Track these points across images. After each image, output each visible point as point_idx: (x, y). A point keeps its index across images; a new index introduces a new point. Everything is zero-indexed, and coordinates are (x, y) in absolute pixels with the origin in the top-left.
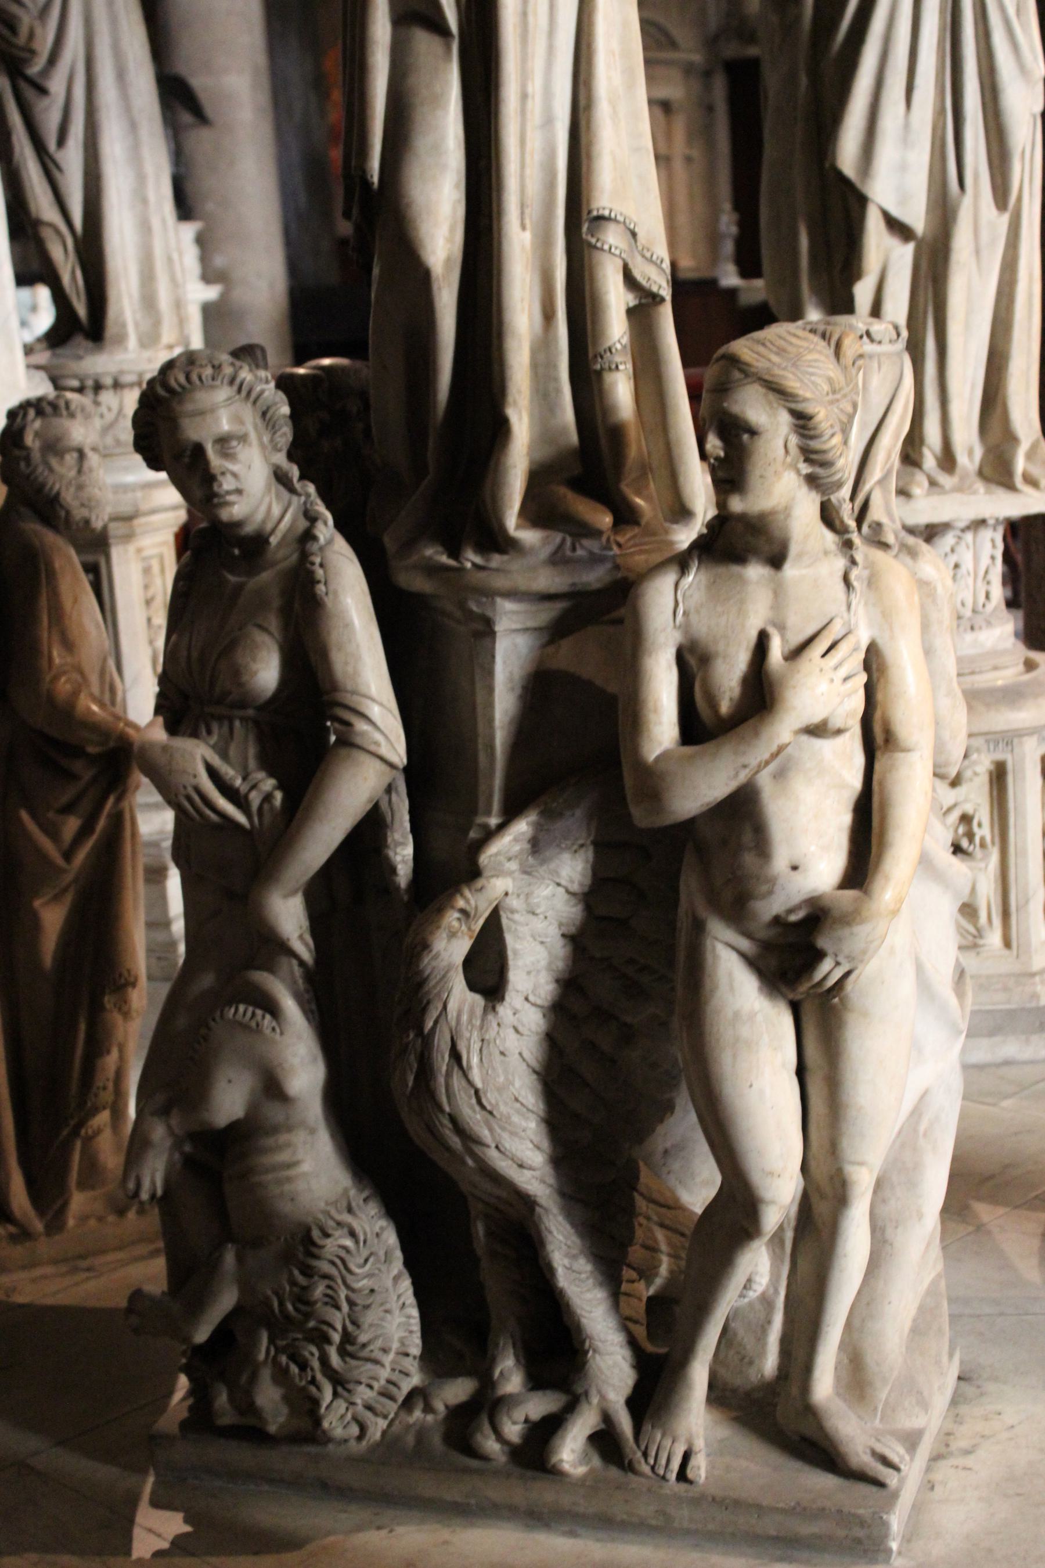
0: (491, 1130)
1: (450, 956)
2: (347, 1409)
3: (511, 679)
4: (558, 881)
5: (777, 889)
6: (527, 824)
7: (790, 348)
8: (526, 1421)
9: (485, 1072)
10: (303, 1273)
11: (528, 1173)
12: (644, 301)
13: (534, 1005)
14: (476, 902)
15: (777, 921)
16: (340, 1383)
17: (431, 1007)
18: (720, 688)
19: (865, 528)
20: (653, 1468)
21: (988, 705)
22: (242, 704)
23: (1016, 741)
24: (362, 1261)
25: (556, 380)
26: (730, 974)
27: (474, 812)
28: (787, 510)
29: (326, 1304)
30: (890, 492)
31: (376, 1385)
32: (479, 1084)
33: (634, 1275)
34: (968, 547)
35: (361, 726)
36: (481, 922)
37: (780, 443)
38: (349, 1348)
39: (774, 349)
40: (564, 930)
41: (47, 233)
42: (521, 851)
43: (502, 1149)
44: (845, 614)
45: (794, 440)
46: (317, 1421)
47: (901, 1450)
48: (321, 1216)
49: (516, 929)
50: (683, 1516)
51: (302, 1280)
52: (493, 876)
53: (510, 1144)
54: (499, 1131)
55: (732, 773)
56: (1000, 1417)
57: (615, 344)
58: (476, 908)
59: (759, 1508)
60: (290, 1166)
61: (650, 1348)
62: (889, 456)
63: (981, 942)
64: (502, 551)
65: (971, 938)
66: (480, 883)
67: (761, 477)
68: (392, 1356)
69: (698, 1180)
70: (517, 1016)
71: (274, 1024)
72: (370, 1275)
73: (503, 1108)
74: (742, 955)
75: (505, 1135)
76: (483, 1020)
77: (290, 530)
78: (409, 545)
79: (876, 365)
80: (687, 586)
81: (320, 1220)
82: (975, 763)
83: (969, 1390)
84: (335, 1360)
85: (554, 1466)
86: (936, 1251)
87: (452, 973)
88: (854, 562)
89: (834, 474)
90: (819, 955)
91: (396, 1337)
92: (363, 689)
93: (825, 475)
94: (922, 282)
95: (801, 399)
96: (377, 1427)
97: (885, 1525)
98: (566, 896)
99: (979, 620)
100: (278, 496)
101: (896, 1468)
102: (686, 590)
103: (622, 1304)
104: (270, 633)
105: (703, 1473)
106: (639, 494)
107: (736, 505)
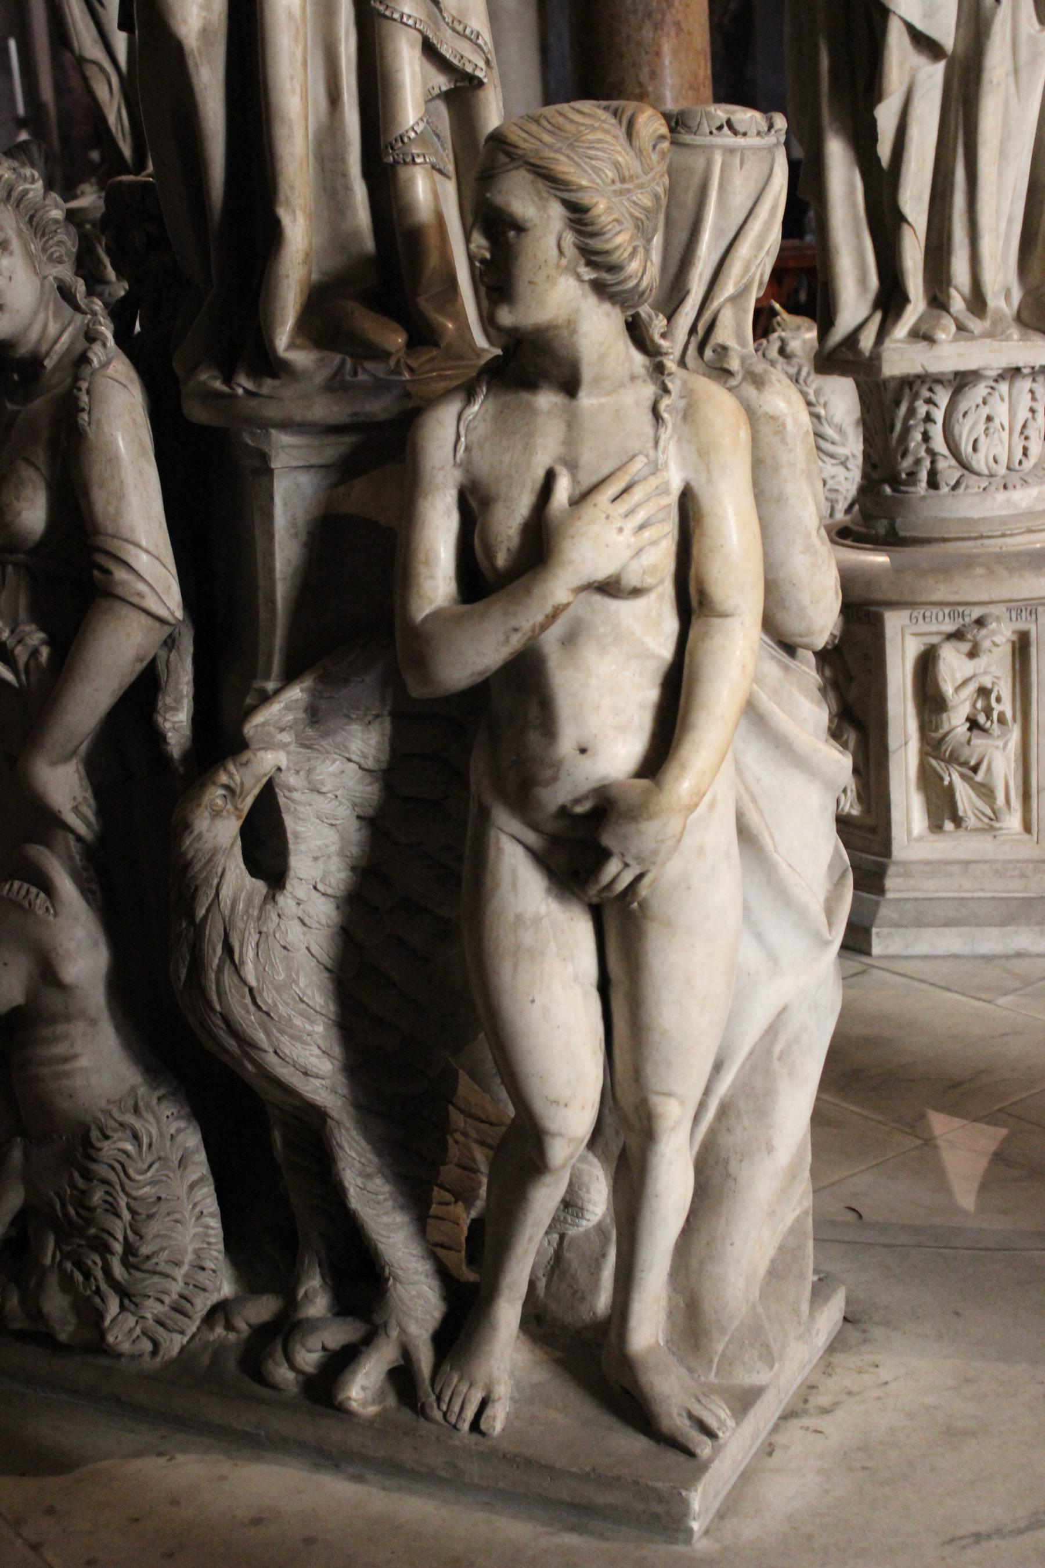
0: (268, 1033)
1: (215, 837)
2: (137, 1322)
3: (294, 525)
4: (347, 755)
6: (302, 691)
7: (569, 127)
9: (261, 968)
10: (83, 1176)
11: (317, 1082)
12: (458, 84)
13: (324, 894)
14: (241, 778)
15: (563, 811)
16: (127, 1296)
18: (497, 537)
19: (708, 353)
20: (445, 1415)
21: (1011, 570)
22: (13, 549)
24: (145, 1166)
26: (514, 871)
28: (571, 325)
29: (106, 1210)
30: (745, 311)
31: (167, 1300)
32: (253, 983)
33: (448, 1197)
34: (1002, 399)
35: (120, 574)
36: (250, 801)
37: (552, 241)
38: (131, 1259)
39: (549, 127)
40: (359, 811)
41: (91, 71)
42: (296, 722)
43: (281, 1054)
44: (652, 453)
45: (569, 238)
46: (102, 1334)
47: (724, 1413)
48: (100, 1115)
49: (296, 809)
50: (473, 1469)
51: (80, 1182)
53: (289, 1047)
54: (278, 1035)
57: (407, 132)
58: (242, 784)
59: (550, 1470)
60: (67, 1059)
62: (747, 269)
63: (997, 825)
64: (274, 375)
65: (986, 820)
66: (246, 756)
67: (531, 283)
68: (185, 1268)
70: (301, 906)
71: (48, 904)
72: (152, 1183)
73: (282, 1010)
74: (527, 848)
75: (284, 1039)
76: (262, 909)
77: (69, 350)
78: (194, 368)
79: (738, 161)
80: (471, 417)
81: (100, 1120)
82: (994, 633)
83: (853, 1334)
84: (118, 1271)
85: (341, 1404)
86: (804, 1184)
87: (221, 859)
88: (666, 390)
90: (604, 855)
91: (190, 1249)
92: (125, 533)
93: (613, 282)
94: (953, 106)
95: (574, 187)
96: (174, 1344)
97: (685, 1503)
98: (360, 773)
99: (1014, 478)
100: (57, 314)
103: (429, 1229)
104: (37, 469)
105: (498, 1426)
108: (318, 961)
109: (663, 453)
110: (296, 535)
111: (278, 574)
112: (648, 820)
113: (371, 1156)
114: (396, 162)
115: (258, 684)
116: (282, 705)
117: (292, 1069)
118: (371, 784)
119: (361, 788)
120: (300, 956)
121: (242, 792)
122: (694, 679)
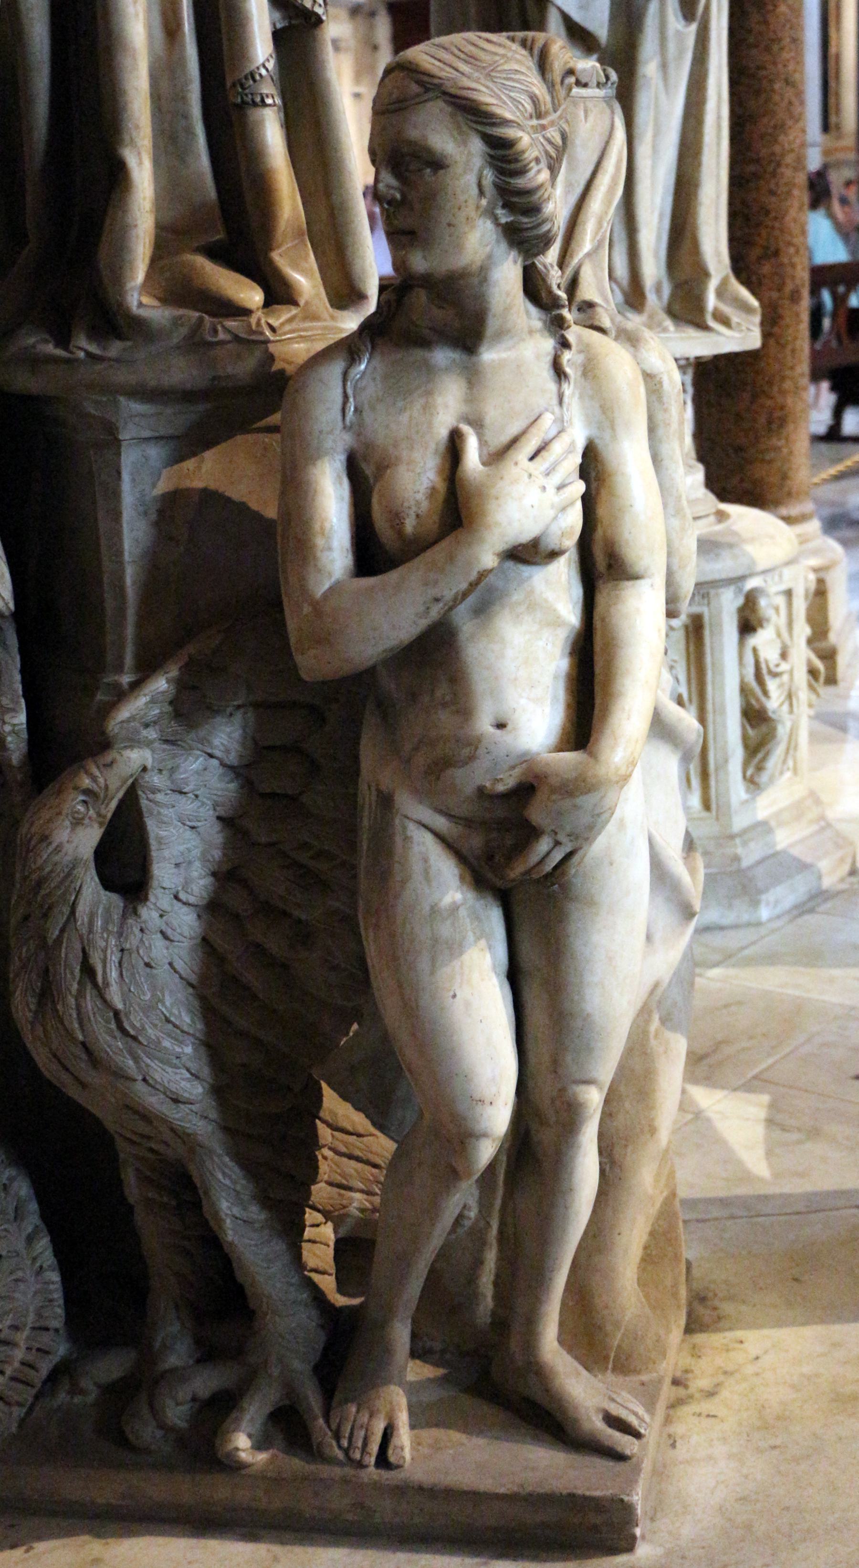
0: (136, 1059)
4: (210, 751)
5: (481, 751)
6: (167, 682)
8: (194, 1399)
9: (126, 988)
14: (106, 780)
15: (481, 792)
17: (56, 911)
20: (346, 1451)
23: (712, 592)
25: (186, 116)
26: (426, 860)
28: (483, 272)
32: (120, 1006)
33: (319, 1218)
36: (114, 804)
37: (471, 179)
39: (462, 56)
40: (221, 811)
43: (151, 1081)
44: (557, 409)
45: (489, 176)
49: (159, 813)
52: (126, 747)
53: (161, 1073)
54: (149, 1061)
55: (422, 609)
56: (742, 1346)
58: (107, 787)
61: (340, 1301)
67: (449, 225)
70: (164, 918)
74: (437, 835)
75: (154, 1064)
79: (582, 114)
87: (79, 871)
88: (565, 344)
89: (539, 225)
90: (532, 833)
93: (529, 226)
98: (221, 770)
101: (637, 1435)
102: (358, 381)
106: (296, 267)
107: (419, 263)
108: (181, 978)
109: (568, 410)
110: (146, 513)
111: (127, 557)
112: (586, 793)
115: (110, 679)
116: (148, 698)
117: (162, 1096)
118: (232, 781)
119: (222, 785)
120: (162, 972)
121: (106, 796)
122: (612, 646)
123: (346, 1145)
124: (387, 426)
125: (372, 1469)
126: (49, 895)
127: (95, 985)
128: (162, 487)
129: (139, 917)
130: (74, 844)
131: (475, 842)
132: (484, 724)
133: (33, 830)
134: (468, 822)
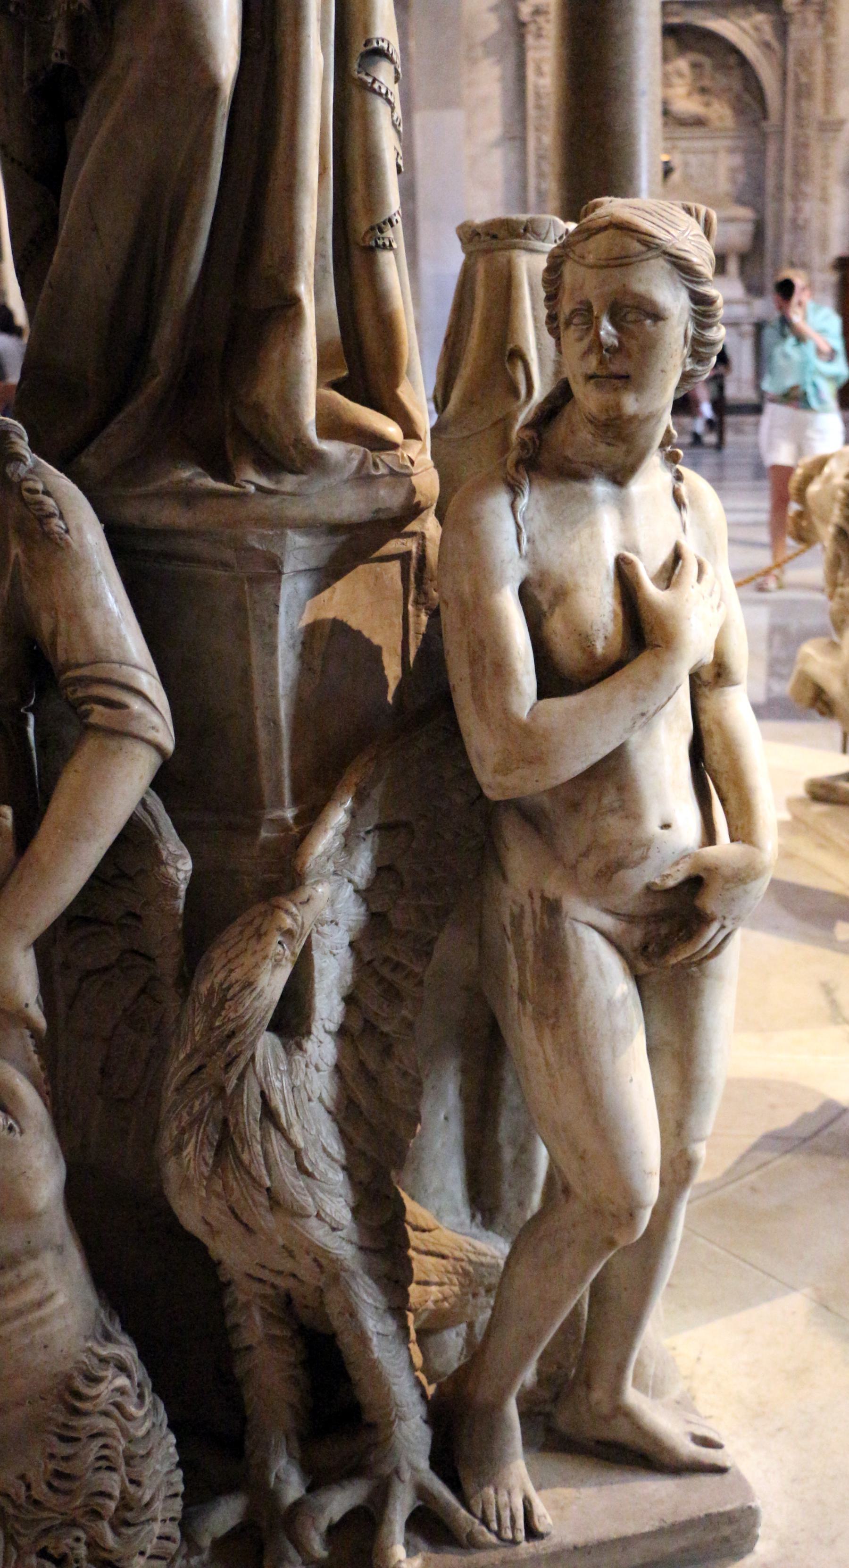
5: (652, 853)
14: (303, 918)
15: (649, 889)
18: (592, 627)
20: (498, 1534)
26: (598, 958)
27: (261, 806)
32: (301, 1144)
38: (129, 1515)
48: (83, 1357)
54: (321, 1195)
58: (303, 923)
69: (431, 1190)
71: (11, 1121)
76: (290, 1063)
110: (294, 646)
112: (755, 879)
113: (380, 1298)
114: (377, 246)
115: (276, 814)
123: (422, 1240)
124: (561, 555)
125: (524, 1544)
126: (242, 1042)
127: (278, 1127)
128: (307, 619)
129: (305, 1051)
130: (273, 987)
131: (637, 935)
132: (652, 826)
133: (234, 976)
134: (630, 919)
